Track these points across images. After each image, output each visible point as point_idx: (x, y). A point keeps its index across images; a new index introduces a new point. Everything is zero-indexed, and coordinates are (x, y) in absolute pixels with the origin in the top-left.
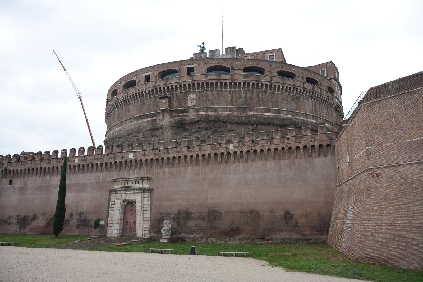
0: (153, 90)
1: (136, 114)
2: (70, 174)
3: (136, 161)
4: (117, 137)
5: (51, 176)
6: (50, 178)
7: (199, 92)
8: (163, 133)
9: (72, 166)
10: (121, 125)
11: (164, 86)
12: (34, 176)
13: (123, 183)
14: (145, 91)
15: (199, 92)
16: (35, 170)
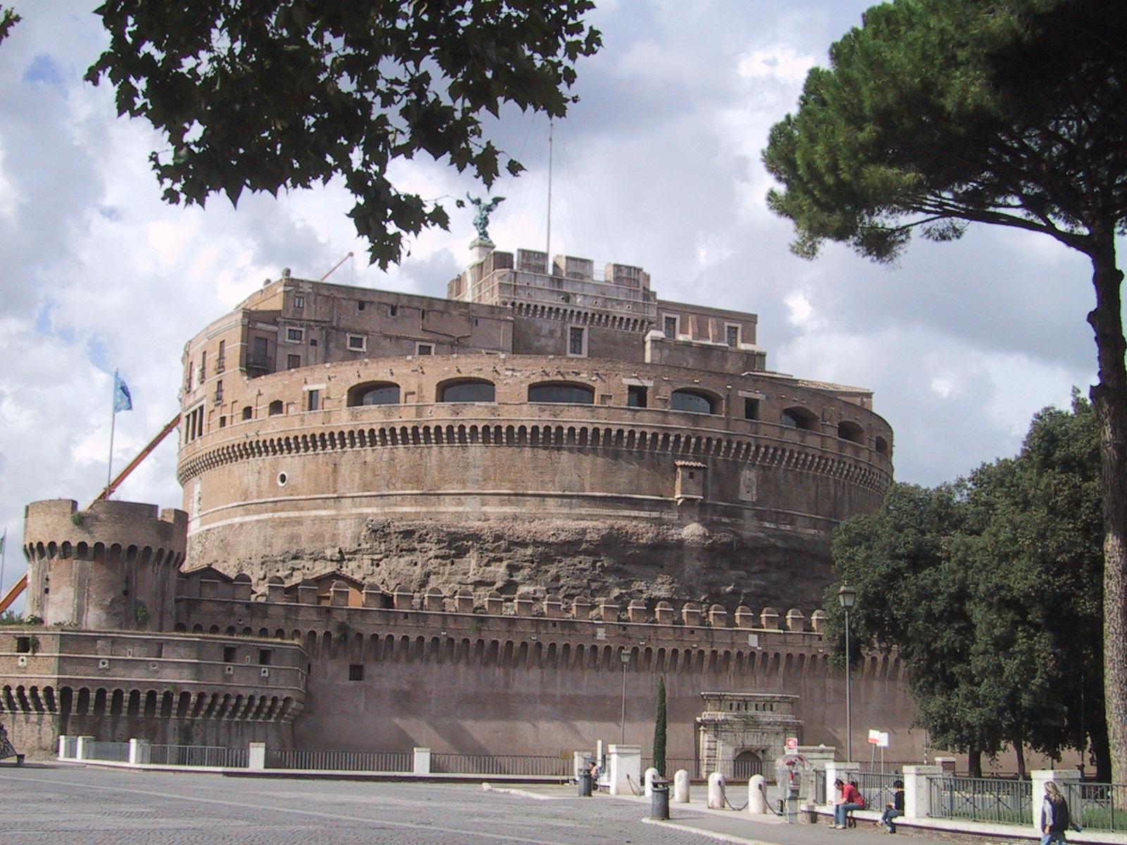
0: (655, 435)
1: (587, 486)
2: (573, 669)
3: (765, 655)
4: (498, 538)
5: (511, 670)
6: (507, 674)
7: (763, 467)
8: (679, 560)
9: (587, 647)
10: (511, 503)
11: (690, 433)
12: (448, 663)
13: (735, 707)
14: (632, 433)
15: (763, 467)
16: (458, 645)
